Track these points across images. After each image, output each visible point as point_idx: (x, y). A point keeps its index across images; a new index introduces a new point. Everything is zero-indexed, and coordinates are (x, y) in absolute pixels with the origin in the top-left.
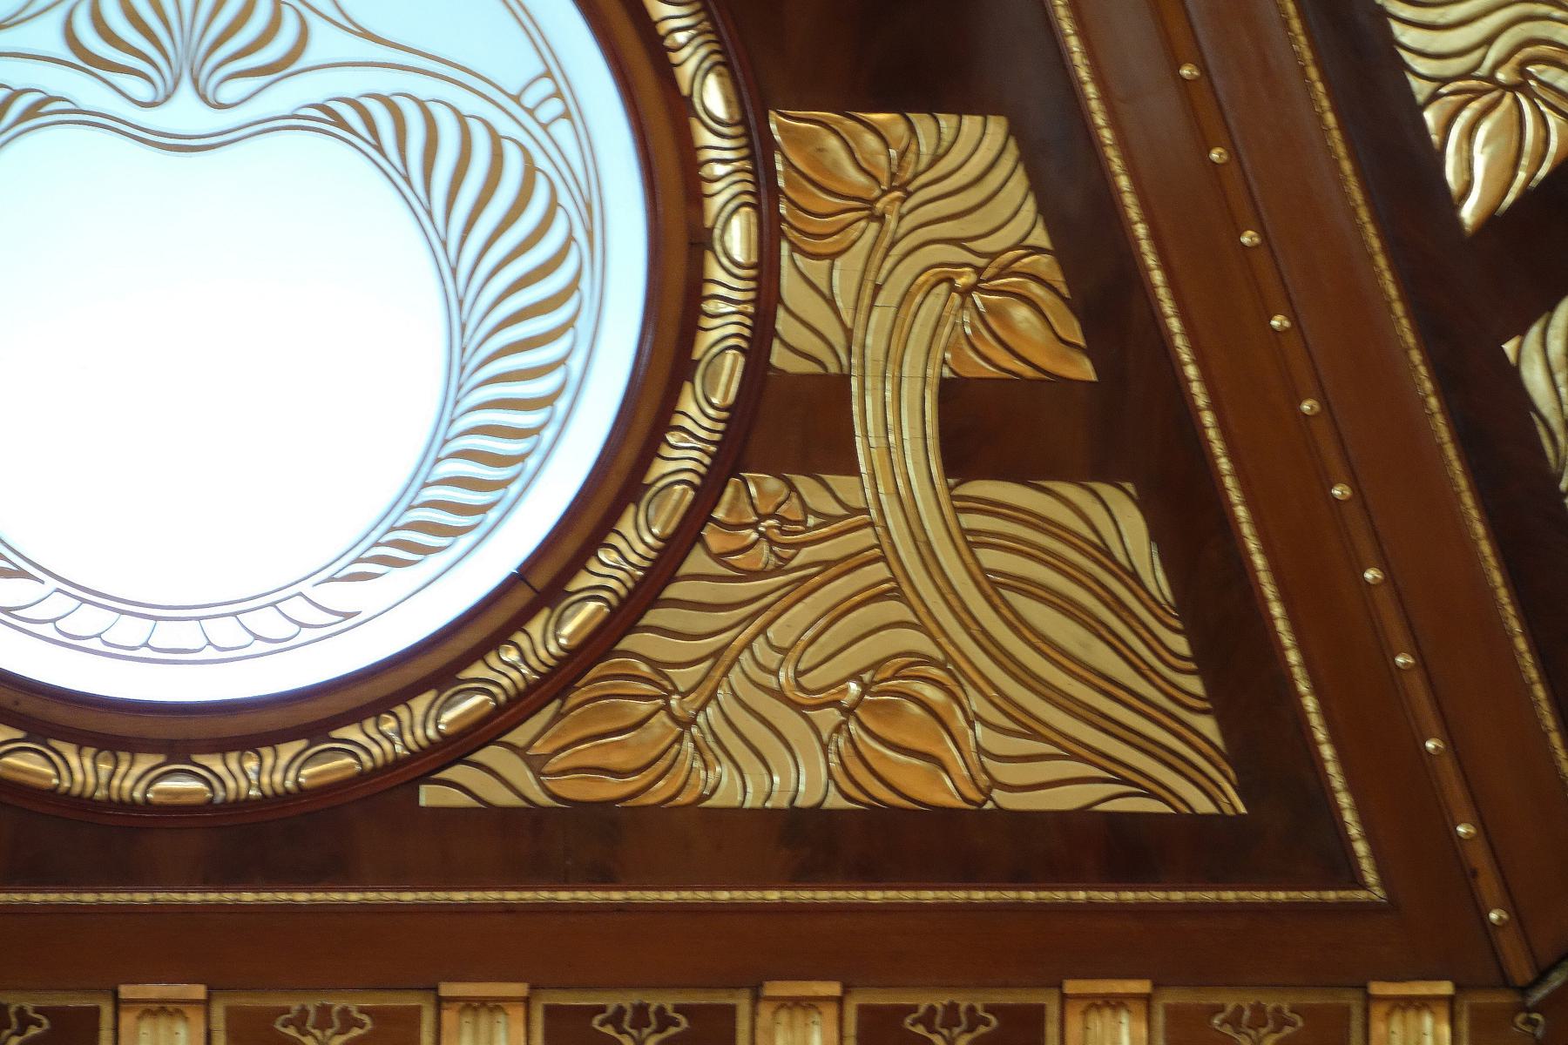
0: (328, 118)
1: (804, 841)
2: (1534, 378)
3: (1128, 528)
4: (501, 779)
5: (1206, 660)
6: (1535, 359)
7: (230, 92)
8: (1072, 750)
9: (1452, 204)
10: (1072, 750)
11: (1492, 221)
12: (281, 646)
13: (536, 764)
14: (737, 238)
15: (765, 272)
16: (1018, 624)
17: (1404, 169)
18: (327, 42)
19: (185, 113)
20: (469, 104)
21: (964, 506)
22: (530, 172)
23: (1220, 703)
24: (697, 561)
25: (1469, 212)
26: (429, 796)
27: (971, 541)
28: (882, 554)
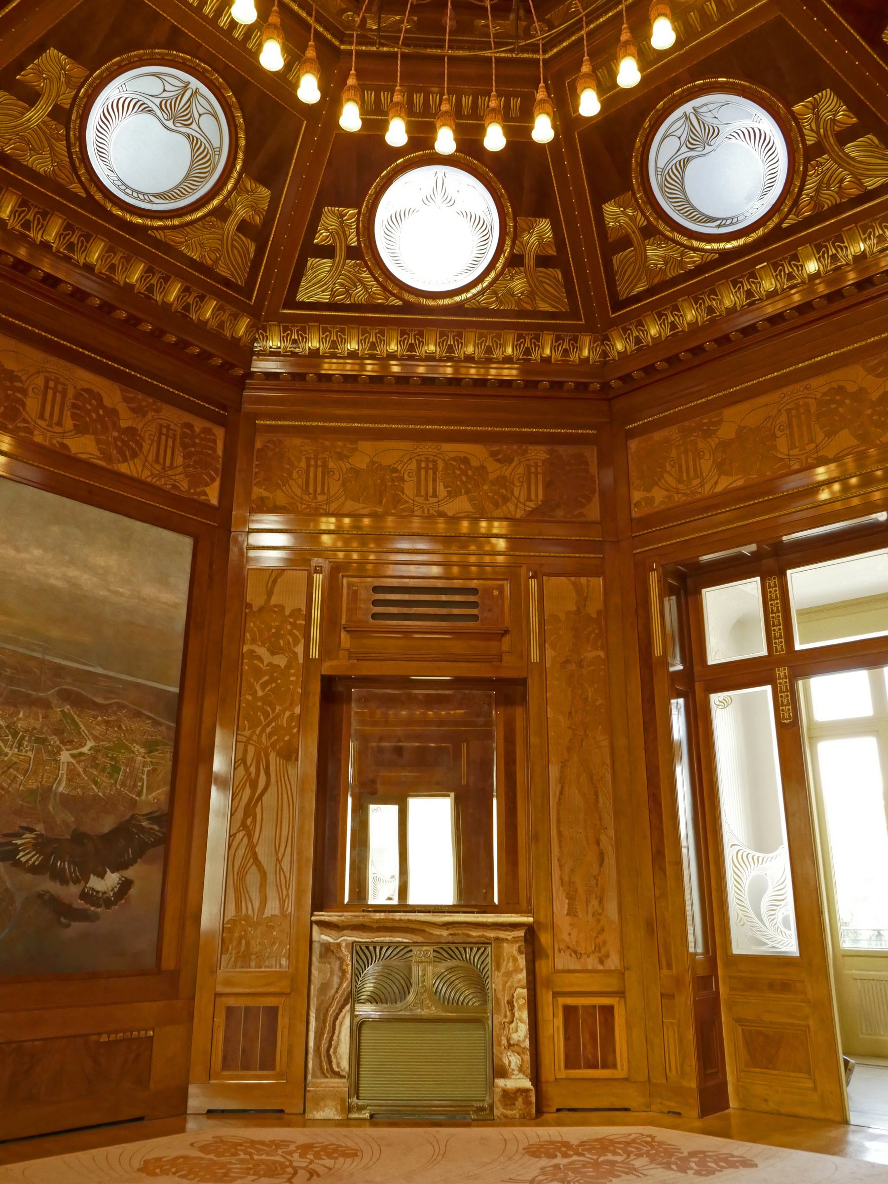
0: (188, 136)
1: (191, 262)
2: (309, 263)
3: (252, 250)
4: (160, 235)
5: (250, 268)
6: (310, 261)
7: (177, 125)
8: (229, 269)
9: (314, 239)
10: (229, 269)
11: (317, 244)
12: (142, 200)
13: (165, 236)
14: (230, 186)
15: (230, 193)
16: (233, 251)
17: (312, 231)
18: (194, 126)
19: (170, 124)
20: (207, 146)
21: (235, 235)
22: (209, 159)
23: (250, 273)
24: (200, 223)
25: (316, 241)
26: (149, 232)
27: (233, 240)
28: (223, 235)
